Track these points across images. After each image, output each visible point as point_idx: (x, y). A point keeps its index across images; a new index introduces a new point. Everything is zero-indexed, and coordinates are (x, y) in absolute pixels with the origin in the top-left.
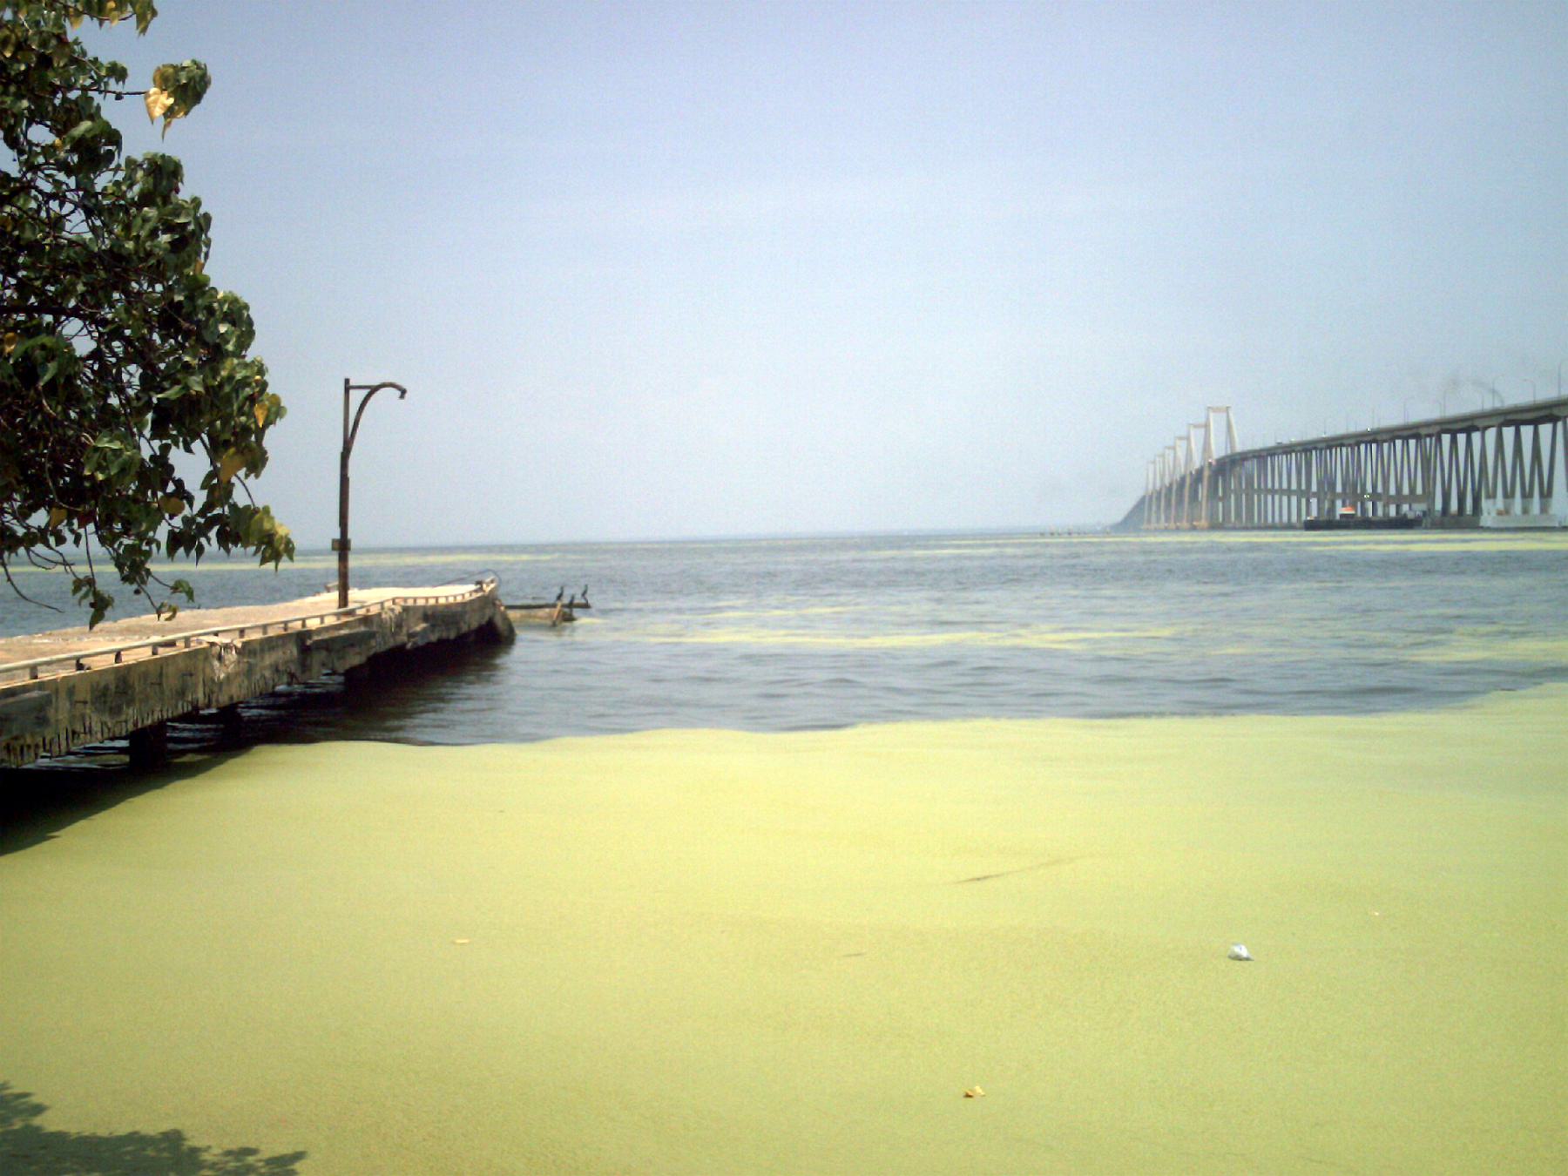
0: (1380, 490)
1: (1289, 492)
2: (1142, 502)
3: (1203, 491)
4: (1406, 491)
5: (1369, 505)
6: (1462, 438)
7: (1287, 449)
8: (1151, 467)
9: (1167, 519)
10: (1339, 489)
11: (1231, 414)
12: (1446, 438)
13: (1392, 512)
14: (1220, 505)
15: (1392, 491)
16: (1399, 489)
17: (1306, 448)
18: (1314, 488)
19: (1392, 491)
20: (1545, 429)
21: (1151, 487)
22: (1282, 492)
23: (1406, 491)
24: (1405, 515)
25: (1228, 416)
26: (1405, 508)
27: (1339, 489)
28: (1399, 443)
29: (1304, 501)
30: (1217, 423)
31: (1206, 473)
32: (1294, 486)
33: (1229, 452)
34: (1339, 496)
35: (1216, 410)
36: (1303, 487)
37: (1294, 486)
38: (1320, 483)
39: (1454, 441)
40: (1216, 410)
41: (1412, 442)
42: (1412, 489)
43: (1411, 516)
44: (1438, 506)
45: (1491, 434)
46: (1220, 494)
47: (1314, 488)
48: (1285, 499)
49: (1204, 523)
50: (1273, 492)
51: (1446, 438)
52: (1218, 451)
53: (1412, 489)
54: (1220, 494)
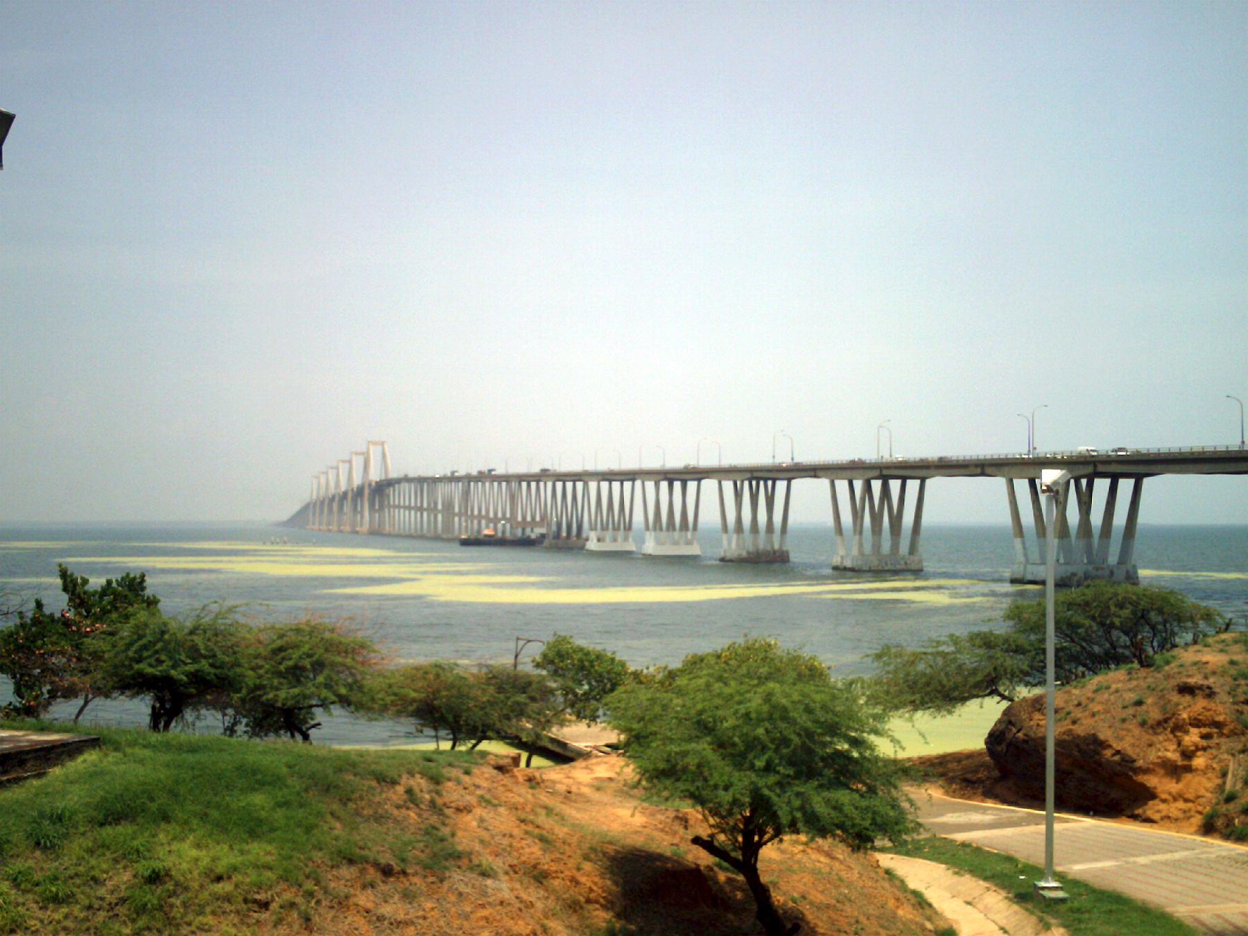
0: (483, 513)
1: (409, 508)
2: (306, 508)
3: (335, 506)
4: (529, 519)
5: (476, 522)
6: (569, 485)
7: (407, 479)
8: (315, 481)
9: (320, 523)
10: (440, 507)
11: (386, 447)
12: (524, 484)
13: (519, 533)
14: (377, 515)
15: (520, 519)
16: (524, 518)
17: (421, 480)
18: (425, 505)
19: (491, 515)
20: (580, 485)
21: (314, 497)
22: (405, 508)
23: (529, 519)
24: (529, 537)
25: (383, 449)
26: (528, 531)
27: (440, 507)
29: (419, 514)
30: (375, 453)
31: (367, 491)
32: (413, 504)
33: (383, 477)
34: (439, 512)
35: (375, 443)
36: (419, 504)
37: (413, 504)
38: (429, 504)
39: (529, 486)
40: (375, 443)
41: (504, 484)
42: (533, 518)
43: (533, 536)
44: (554, 528)
45: (550, 484)
46: (377, 507)
47: (425, 505)
48: (407, 512)
49: (348, 528)
50: (399, 507)
51: (524, 484)
52: (375, 476)
53: (533, 518)
54: (377, 507)
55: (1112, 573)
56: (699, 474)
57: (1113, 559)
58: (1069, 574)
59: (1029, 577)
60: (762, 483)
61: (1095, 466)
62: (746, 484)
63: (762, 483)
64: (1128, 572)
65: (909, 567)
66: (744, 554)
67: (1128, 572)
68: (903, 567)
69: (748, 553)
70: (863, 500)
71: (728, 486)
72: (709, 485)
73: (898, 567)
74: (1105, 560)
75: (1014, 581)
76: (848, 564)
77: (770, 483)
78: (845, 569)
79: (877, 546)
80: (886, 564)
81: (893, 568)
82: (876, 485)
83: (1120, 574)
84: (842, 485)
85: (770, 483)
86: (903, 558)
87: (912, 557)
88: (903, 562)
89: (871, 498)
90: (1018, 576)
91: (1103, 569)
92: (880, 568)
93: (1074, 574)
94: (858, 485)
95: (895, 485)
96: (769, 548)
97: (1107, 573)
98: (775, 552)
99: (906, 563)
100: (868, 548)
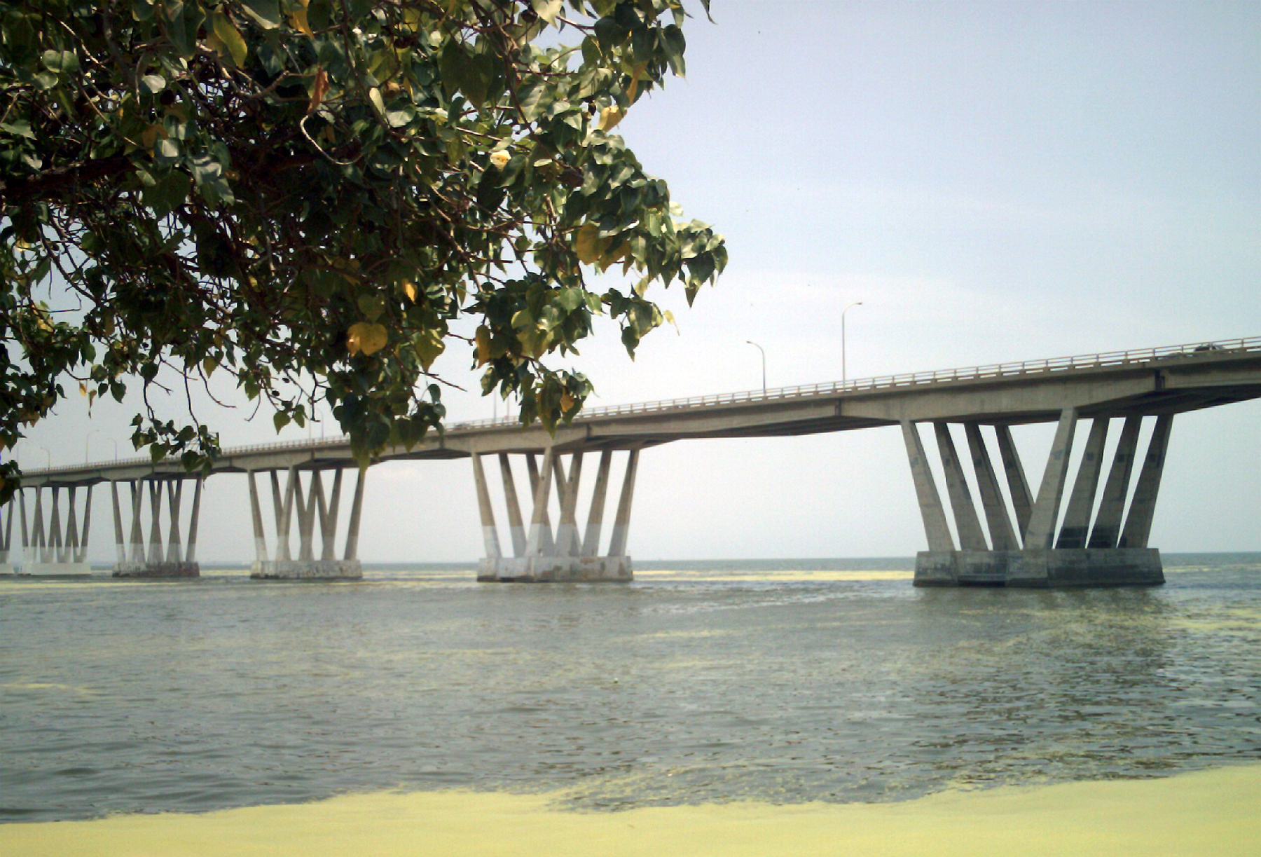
28: (64, 492)
55: (603, 566)
56: (90, 476)
57: (603, 550)
58: (552, 569)
59: (503, 574)
60: (165, 484)
61: (589, 429)
62: (146, 484)
63: (165, 484)
64: (621, 565)
65: (346, 574)
66: (143, 568)
67: (621, 565)
68: (339, 574)
69: (148, 566)
70: (289, 492)
71: (124, 488)
72: (102, 490)
73: (332, 574)
74: (594, 550)
75: (480, 579)
76: (270, 571)
77: (175, 483)
78: (267, 577)
79: (306, 549)
80: (318, 571)
81: (324, 575)
82: (306, 477)
83: (612, 571)
84: (263, 479)
85: (175, 483)
86: (338, 563)
87: (348, 563)
88: (337, 568)
89: (299, 493)
90: (489, 573)
91: (592, 561)
92: (311, 575)
93: (558, 568)
94: (283, 477)
95: (327, 476)
96: (173, 560)
97: (597, 567)
98: (180, 565)
99: (341, 569)
100: (295, 554)
